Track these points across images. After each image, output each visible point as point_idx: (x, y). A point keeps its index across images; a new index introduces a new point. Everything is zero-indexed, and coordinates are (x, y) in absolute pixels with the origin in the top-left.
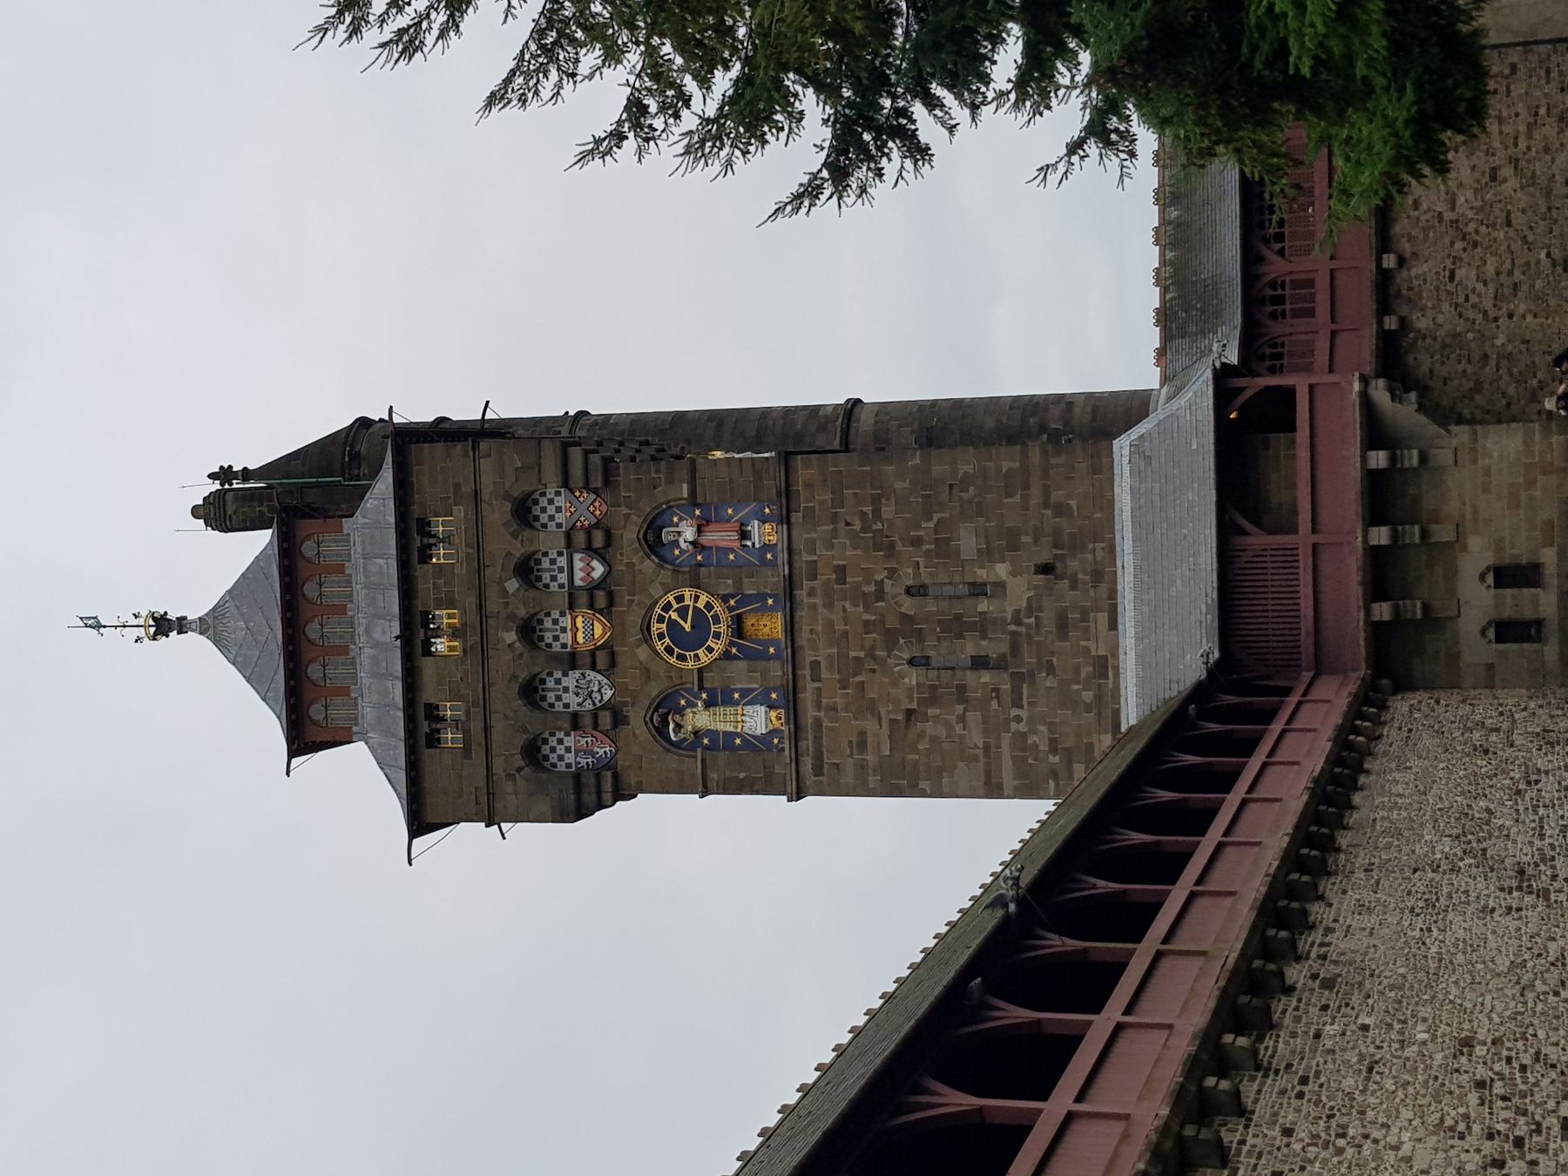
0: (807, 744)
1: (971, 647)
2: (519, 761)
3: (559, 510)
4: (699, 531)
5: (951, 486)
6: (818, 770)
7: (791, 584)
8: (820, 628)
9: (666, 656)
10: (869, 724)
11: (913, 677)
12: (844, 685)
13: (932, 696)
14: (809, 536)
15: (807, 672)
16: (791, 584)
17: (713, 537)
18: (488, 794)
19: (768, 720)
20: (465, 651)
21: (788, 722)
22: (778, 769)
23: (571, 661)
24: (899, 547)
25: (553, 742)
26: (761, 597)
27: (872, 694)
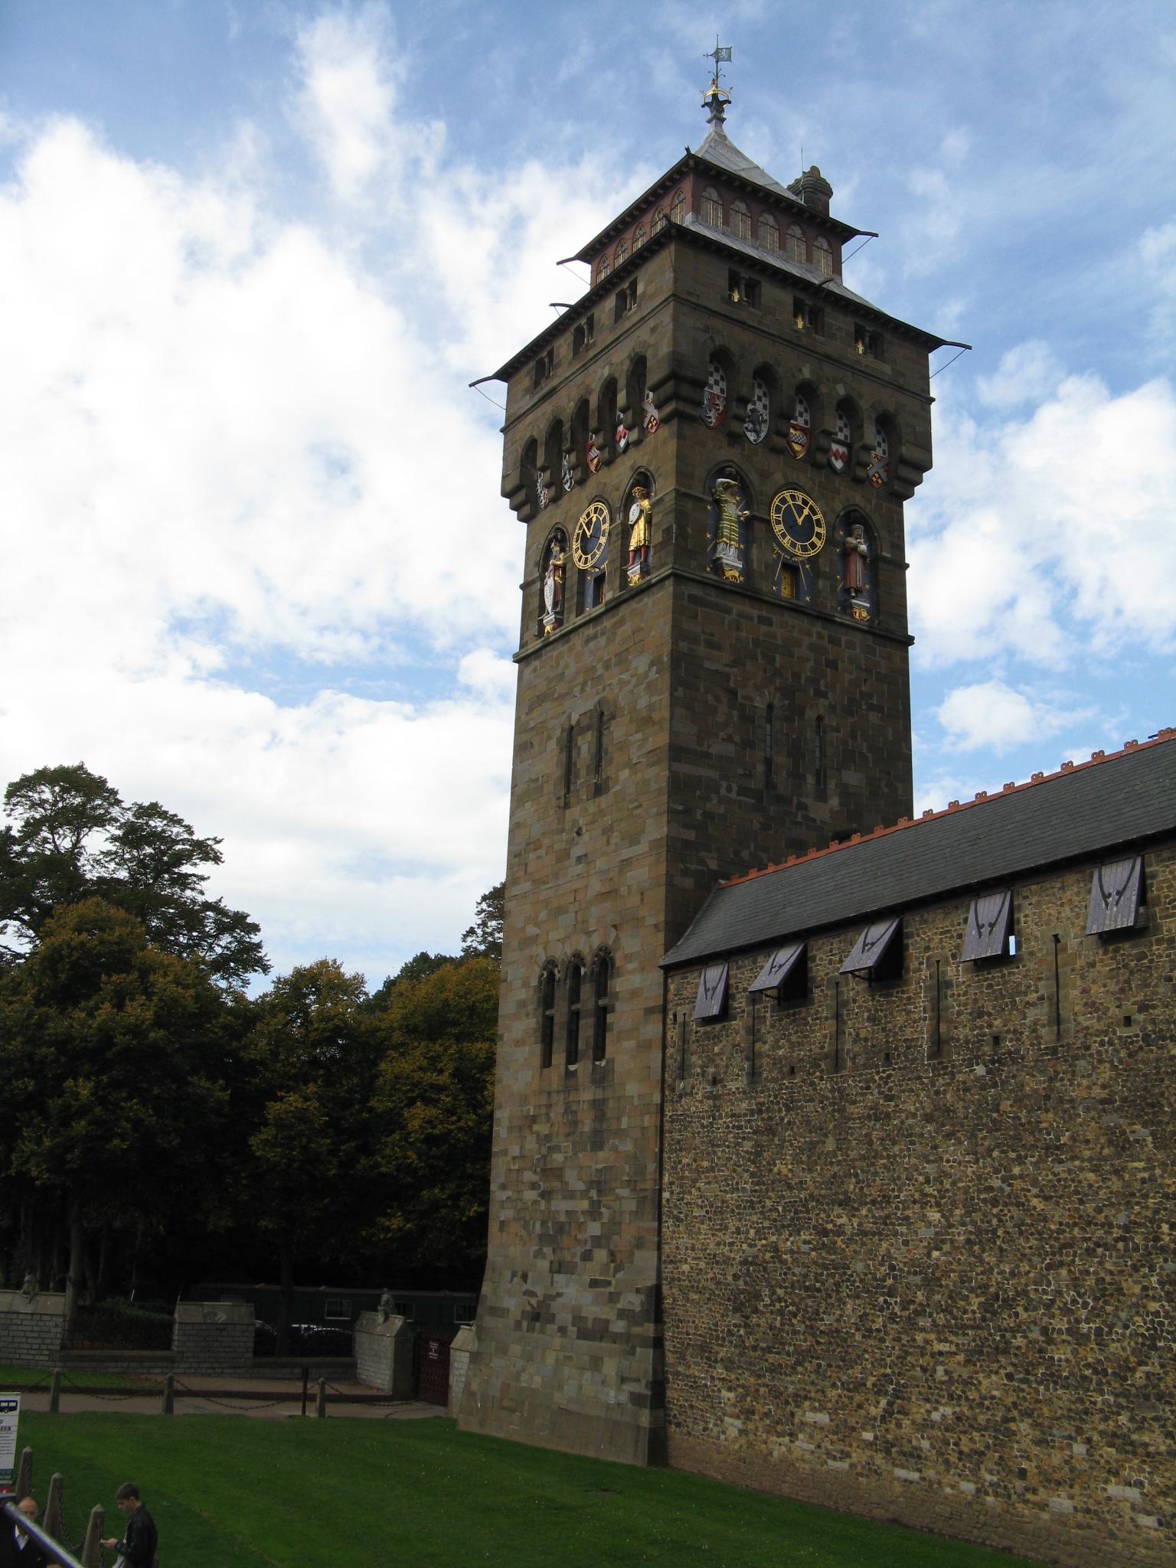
0: (713, 597)
1: (781, 760)
4: (863, 557)
5: (889, 773)
6: (693, 599)
7: (827, 620)
8: (795, 635)
11: (760, 703)
12: (756, 642)
14: (858, 646)
15: (764, 613)
16: (827, 620)
18: (697, 305)
20: (797, 331)
21: (732, 584)
22: (694, 563)
23: (782, 416)
24: (851, 720)
25: (716, 376)
26: (814, 592)
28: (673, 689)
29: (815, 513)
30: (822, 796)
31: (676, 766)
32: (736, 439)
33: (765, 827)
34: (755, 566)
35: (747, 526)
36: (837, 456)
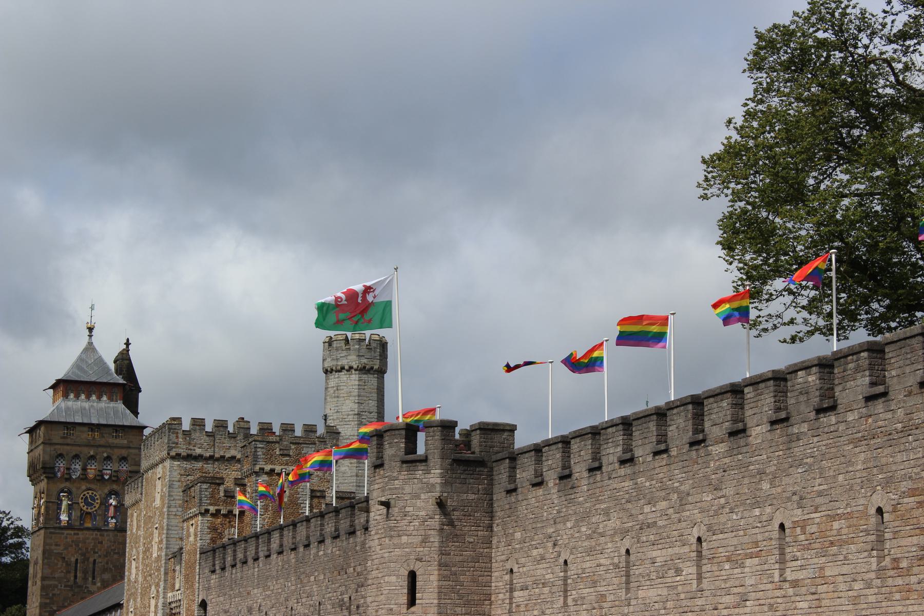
2: (59, 452)
3: (123, 467)
4: (115, 506)
6: (51, 533)
7: (99, 530)
9: (83, 494)
10: (62, 548)
11: (73, 559)
12: (72, 541)
13: (68, 564)
16: (99, 530)
17: (112, 509)
19: (65, 520)
22: (52, 522)
23: (84, 469)
24: (106, 558)
27: (70, 549)
28: (43, 560)
29: (95, 495)
30: (94, 583)
31: (43, 582)
32: (69, 479)
33: (73, 595)
34: (73, 518)
35: (70, 507)
36: (107, 474)
